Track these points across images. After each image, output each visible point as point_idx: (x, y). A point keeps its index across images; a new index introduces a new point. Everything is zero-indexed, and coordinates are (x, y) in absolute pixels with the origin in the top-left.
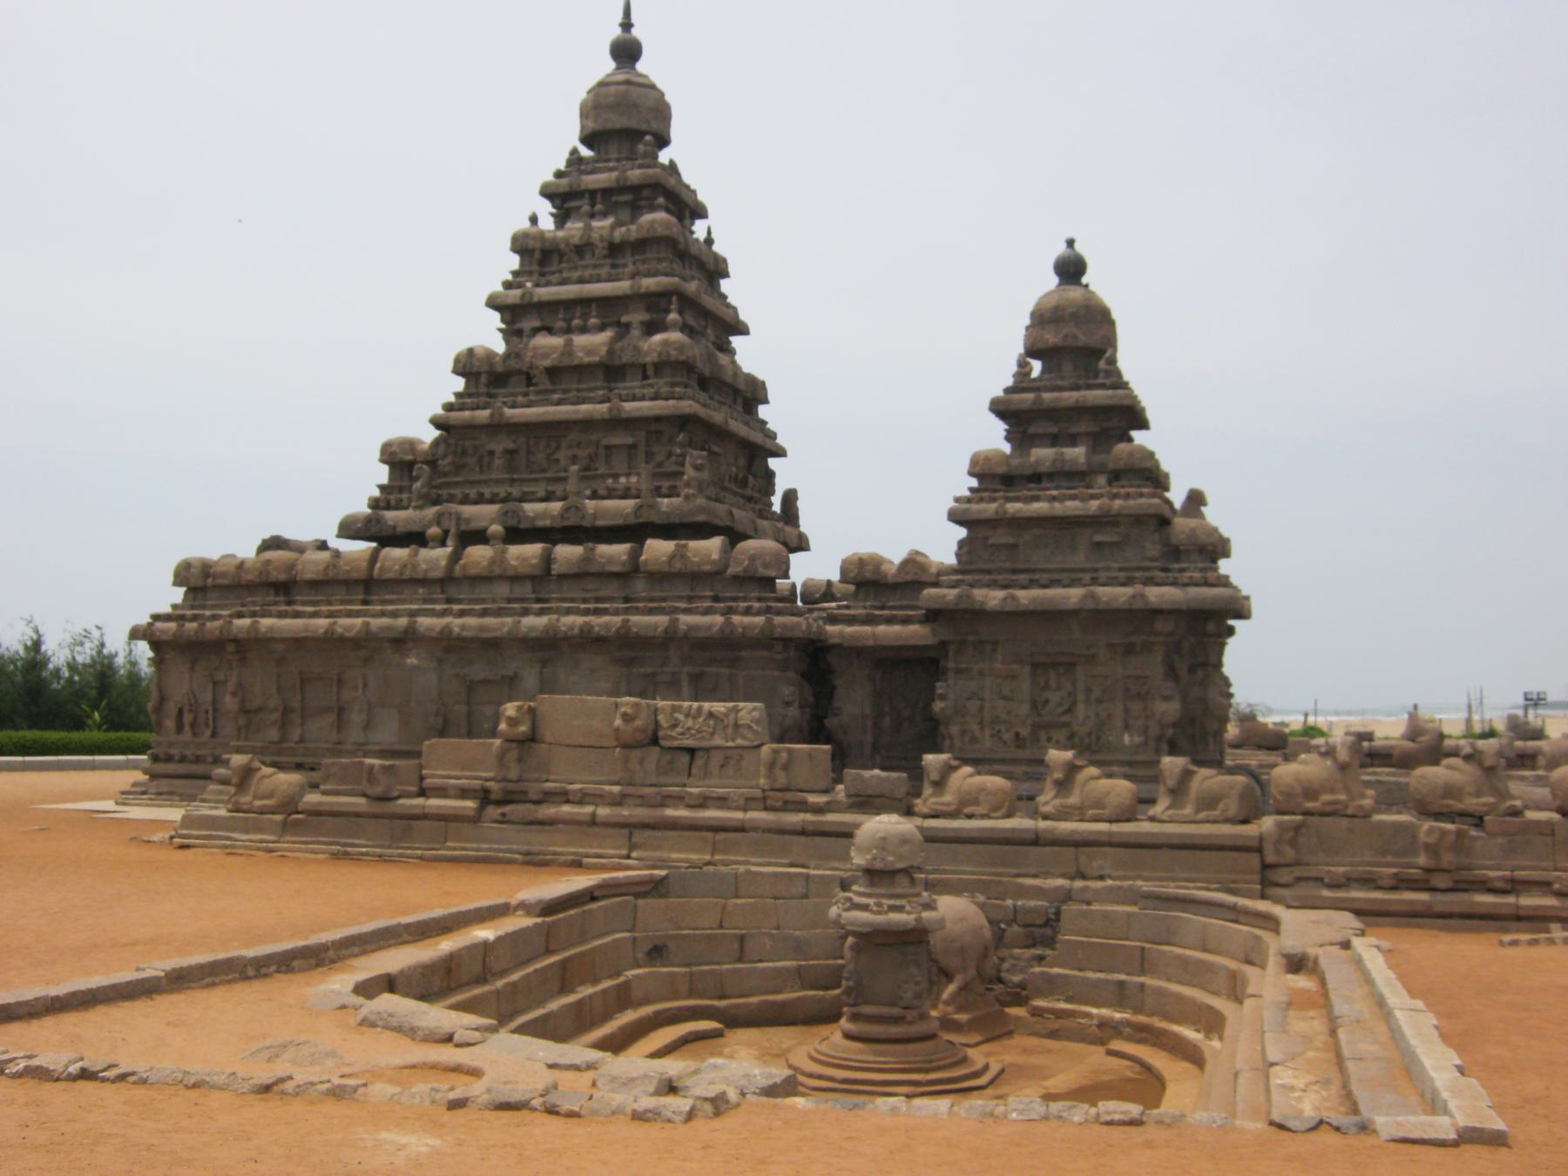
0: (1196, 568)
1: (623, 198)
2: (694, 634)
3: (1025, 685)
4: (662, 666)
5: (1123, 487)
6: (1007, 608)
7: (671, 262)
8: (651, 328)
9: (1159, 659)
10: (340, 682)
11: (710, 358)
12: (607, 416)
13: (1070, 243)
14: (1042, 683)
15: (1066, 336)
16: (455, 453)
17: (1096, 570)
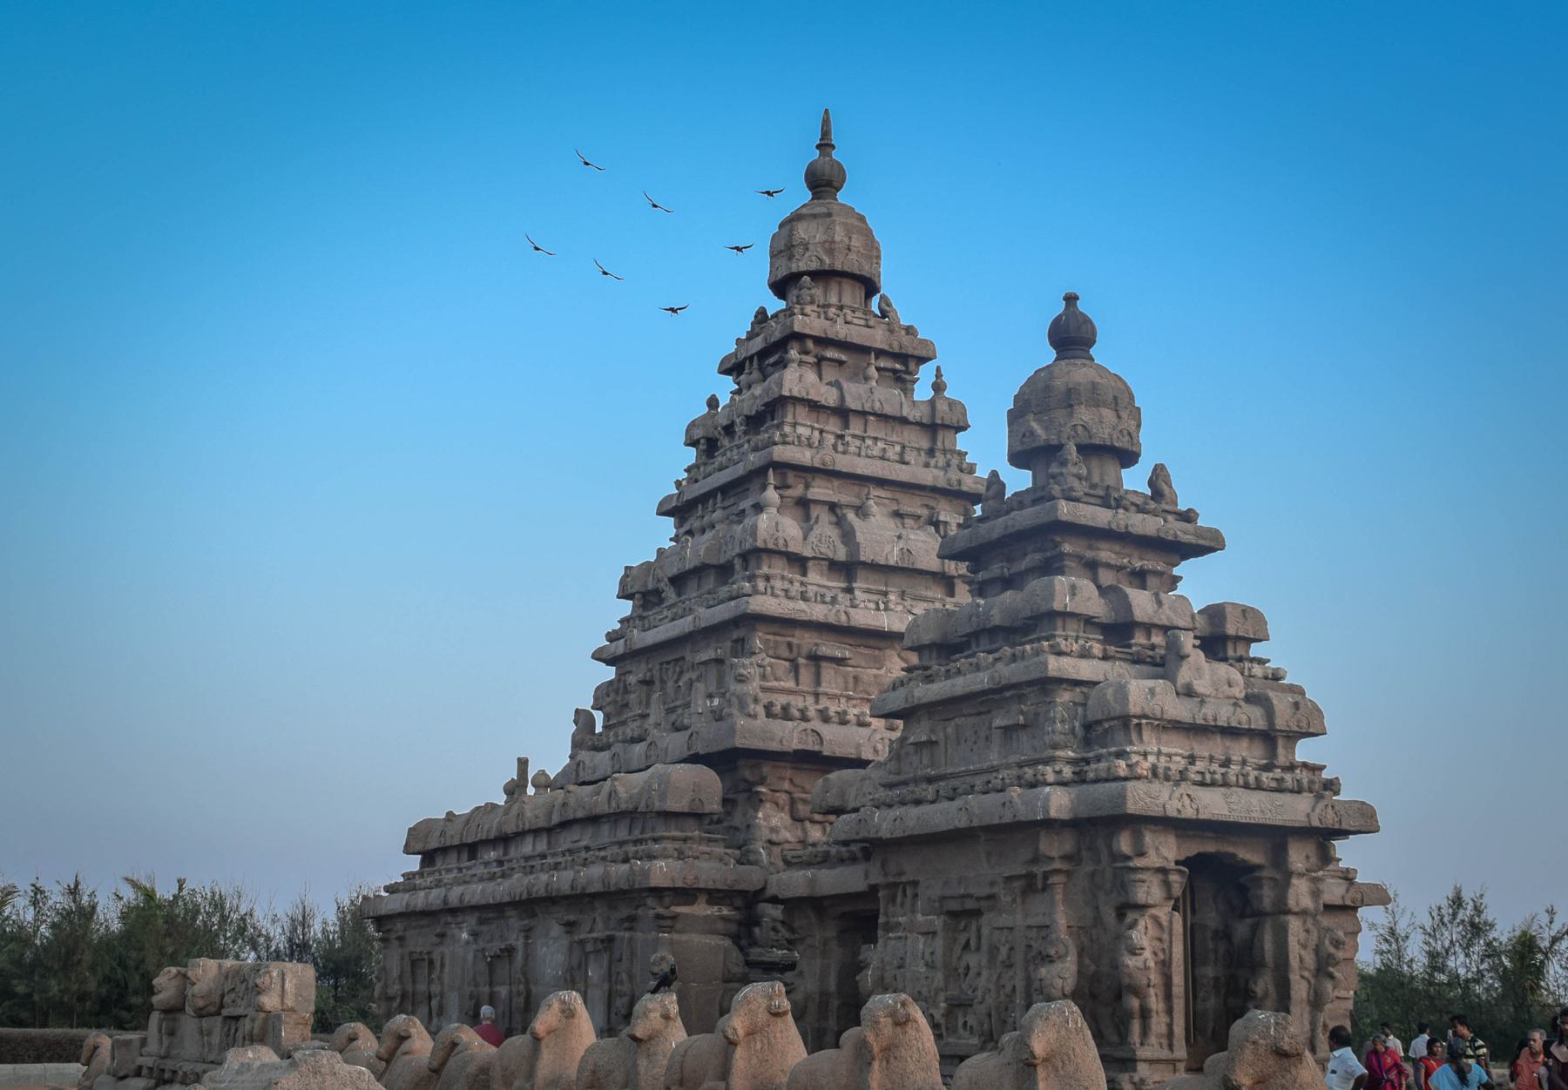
0: (1110, 754)
1: (772, 360)
2: (591, 890)
3: (939, 943)
4: (591, 931)
5: (1031, 642)
6: (898, 834)
7: (794, 425)
8: (759, 508)
9: (1059, 897)
10: (431, 962)
11: (848, 536)
12: (692, 629)
13: (1071, 299)
14: (963, 942)
15: (1024, 435)
16: (617, 692)
17: (995, 769)
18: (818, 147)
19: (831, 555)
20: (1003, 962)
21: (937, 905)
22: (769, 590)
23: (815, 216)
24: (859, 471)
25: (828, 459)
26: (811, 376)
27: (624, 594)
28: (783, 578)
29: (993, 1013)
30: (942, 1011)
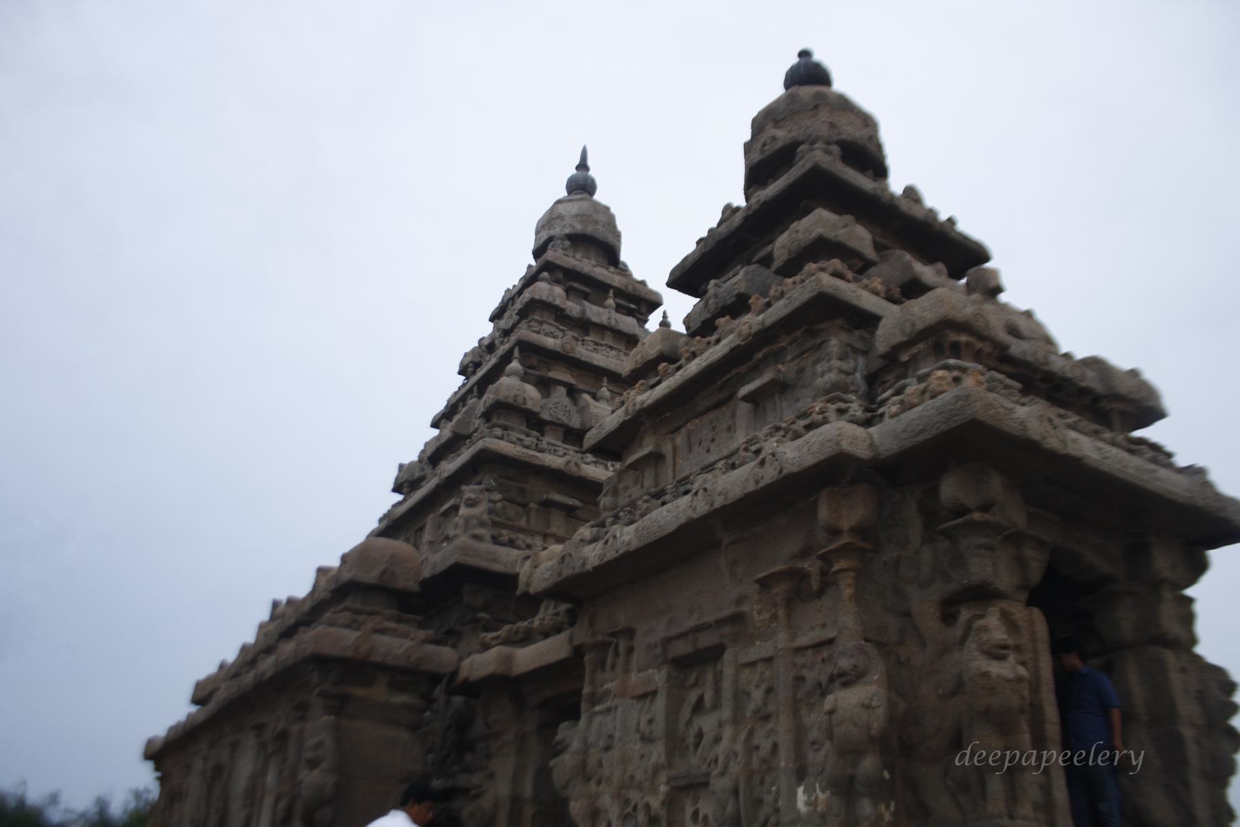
7: (541, 323)
9: (848, 592)
11: (582, 410)
14: (693, 697)
15: (764, 145)
18: (578, 168)
19: (566, 421)
20: (756, 712)
21: (658, 651)
22: (505, 437)
23: (570, 201)
24: (596, 363)
25: (568, 347)
26: (559, 290)
27: (396, 489)
28: (521, 432)
29: (742, 788)
30: (661, 797)
